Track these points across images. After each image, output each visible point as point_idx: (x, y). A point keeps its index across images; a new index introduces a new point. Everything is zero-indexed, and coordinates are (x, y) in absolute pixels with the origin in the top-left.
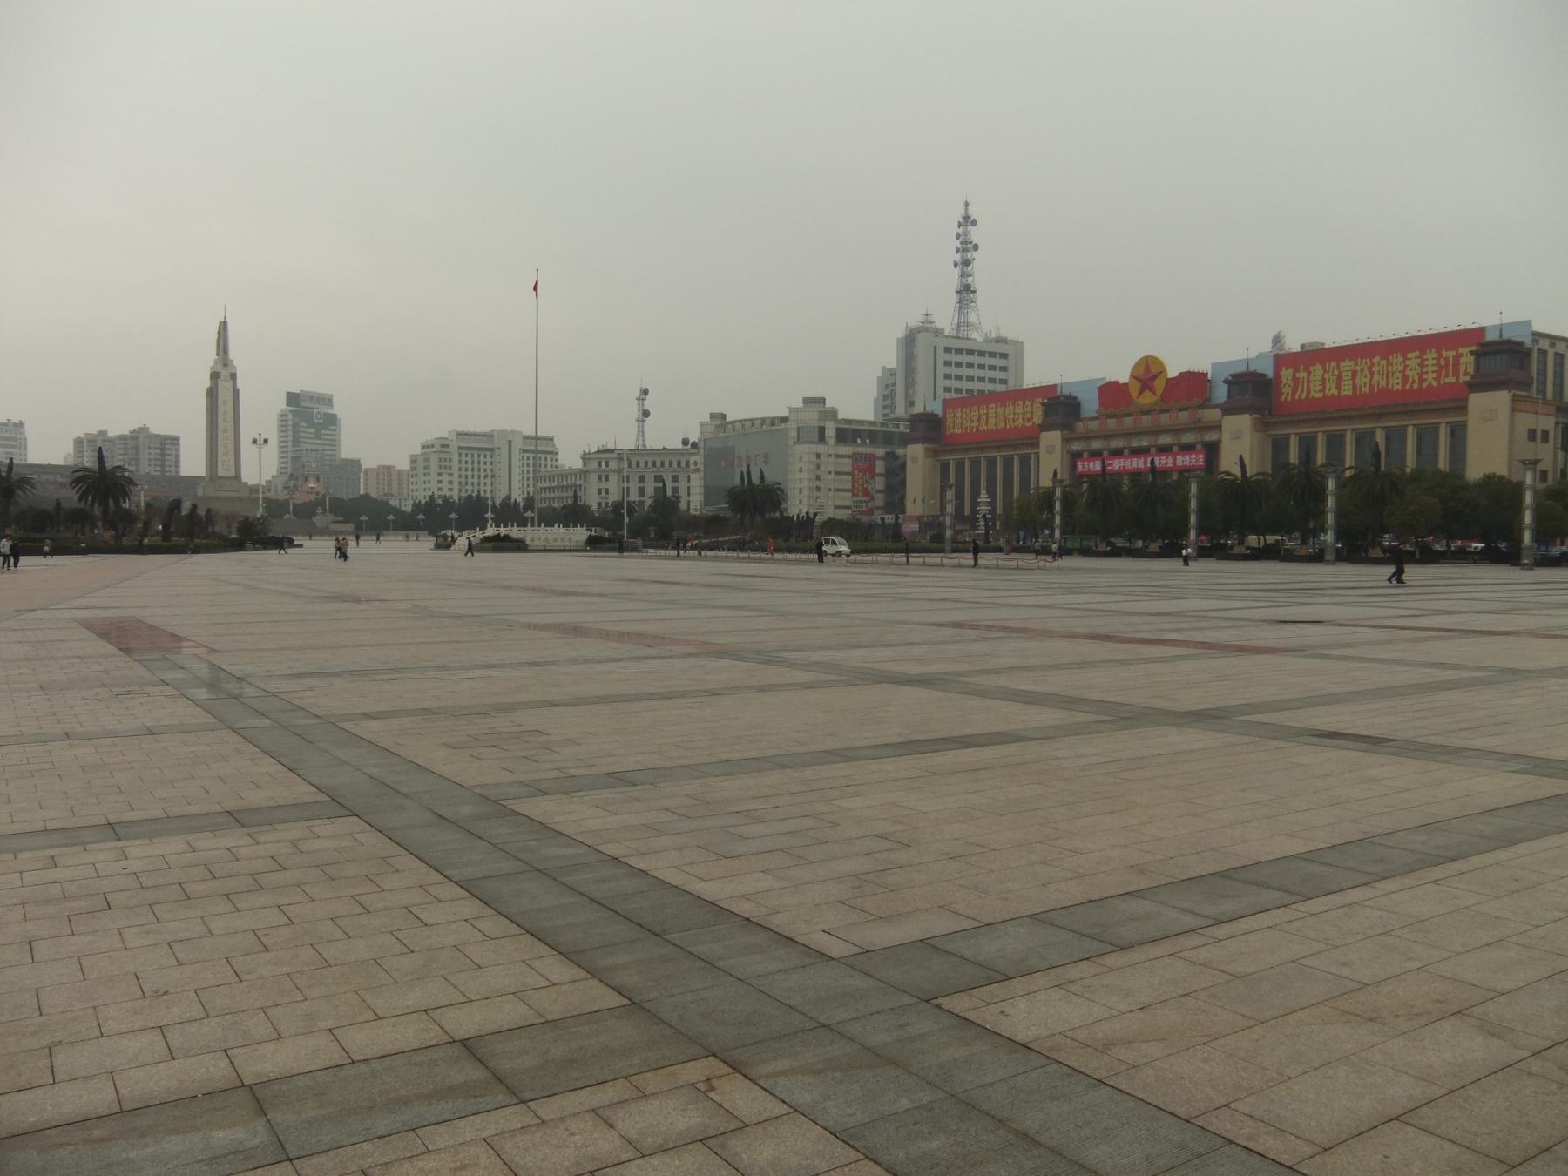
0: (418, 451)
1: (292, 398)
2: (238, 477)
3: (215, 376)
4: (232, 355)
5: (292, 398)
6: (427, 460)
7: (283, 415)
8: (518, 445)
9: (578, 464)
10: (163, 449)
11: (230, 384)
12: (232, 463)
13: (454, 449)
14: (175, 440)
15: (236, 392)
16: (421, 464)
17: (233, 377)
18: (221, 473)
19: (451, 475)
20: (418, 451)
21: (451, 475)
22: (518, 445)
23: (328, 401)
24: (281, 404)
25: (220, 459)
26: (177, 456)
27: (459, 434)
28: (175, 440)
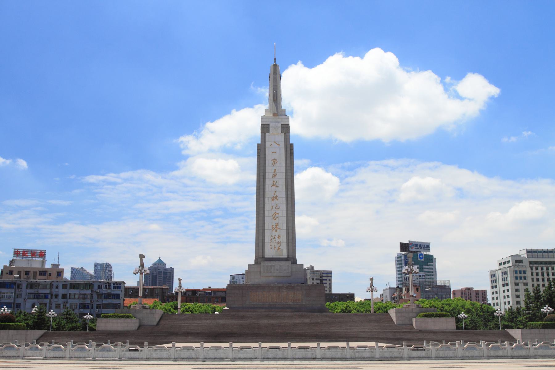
0: (497, 267)
1: (404, 247)
2: (291, 259)
3: (265, 128)
4: (285, 103)
5: (404, 247)
6: (504, 273)
7: (399, 257)
10: (321, 280)
11: (281, 138)
12: (284, 239)
13: (526, 263)
14: (328, 274)
15: (289, 150)
16: (499, 277)
17: (286, 128)
18: (269, 253)
19: (526, 284)
20: (497, 267)
21: (526, 284)
23: (427, 247)
24: (398, 250)
25: (267, 233)
27: (528, 252)
28: (328, 274)
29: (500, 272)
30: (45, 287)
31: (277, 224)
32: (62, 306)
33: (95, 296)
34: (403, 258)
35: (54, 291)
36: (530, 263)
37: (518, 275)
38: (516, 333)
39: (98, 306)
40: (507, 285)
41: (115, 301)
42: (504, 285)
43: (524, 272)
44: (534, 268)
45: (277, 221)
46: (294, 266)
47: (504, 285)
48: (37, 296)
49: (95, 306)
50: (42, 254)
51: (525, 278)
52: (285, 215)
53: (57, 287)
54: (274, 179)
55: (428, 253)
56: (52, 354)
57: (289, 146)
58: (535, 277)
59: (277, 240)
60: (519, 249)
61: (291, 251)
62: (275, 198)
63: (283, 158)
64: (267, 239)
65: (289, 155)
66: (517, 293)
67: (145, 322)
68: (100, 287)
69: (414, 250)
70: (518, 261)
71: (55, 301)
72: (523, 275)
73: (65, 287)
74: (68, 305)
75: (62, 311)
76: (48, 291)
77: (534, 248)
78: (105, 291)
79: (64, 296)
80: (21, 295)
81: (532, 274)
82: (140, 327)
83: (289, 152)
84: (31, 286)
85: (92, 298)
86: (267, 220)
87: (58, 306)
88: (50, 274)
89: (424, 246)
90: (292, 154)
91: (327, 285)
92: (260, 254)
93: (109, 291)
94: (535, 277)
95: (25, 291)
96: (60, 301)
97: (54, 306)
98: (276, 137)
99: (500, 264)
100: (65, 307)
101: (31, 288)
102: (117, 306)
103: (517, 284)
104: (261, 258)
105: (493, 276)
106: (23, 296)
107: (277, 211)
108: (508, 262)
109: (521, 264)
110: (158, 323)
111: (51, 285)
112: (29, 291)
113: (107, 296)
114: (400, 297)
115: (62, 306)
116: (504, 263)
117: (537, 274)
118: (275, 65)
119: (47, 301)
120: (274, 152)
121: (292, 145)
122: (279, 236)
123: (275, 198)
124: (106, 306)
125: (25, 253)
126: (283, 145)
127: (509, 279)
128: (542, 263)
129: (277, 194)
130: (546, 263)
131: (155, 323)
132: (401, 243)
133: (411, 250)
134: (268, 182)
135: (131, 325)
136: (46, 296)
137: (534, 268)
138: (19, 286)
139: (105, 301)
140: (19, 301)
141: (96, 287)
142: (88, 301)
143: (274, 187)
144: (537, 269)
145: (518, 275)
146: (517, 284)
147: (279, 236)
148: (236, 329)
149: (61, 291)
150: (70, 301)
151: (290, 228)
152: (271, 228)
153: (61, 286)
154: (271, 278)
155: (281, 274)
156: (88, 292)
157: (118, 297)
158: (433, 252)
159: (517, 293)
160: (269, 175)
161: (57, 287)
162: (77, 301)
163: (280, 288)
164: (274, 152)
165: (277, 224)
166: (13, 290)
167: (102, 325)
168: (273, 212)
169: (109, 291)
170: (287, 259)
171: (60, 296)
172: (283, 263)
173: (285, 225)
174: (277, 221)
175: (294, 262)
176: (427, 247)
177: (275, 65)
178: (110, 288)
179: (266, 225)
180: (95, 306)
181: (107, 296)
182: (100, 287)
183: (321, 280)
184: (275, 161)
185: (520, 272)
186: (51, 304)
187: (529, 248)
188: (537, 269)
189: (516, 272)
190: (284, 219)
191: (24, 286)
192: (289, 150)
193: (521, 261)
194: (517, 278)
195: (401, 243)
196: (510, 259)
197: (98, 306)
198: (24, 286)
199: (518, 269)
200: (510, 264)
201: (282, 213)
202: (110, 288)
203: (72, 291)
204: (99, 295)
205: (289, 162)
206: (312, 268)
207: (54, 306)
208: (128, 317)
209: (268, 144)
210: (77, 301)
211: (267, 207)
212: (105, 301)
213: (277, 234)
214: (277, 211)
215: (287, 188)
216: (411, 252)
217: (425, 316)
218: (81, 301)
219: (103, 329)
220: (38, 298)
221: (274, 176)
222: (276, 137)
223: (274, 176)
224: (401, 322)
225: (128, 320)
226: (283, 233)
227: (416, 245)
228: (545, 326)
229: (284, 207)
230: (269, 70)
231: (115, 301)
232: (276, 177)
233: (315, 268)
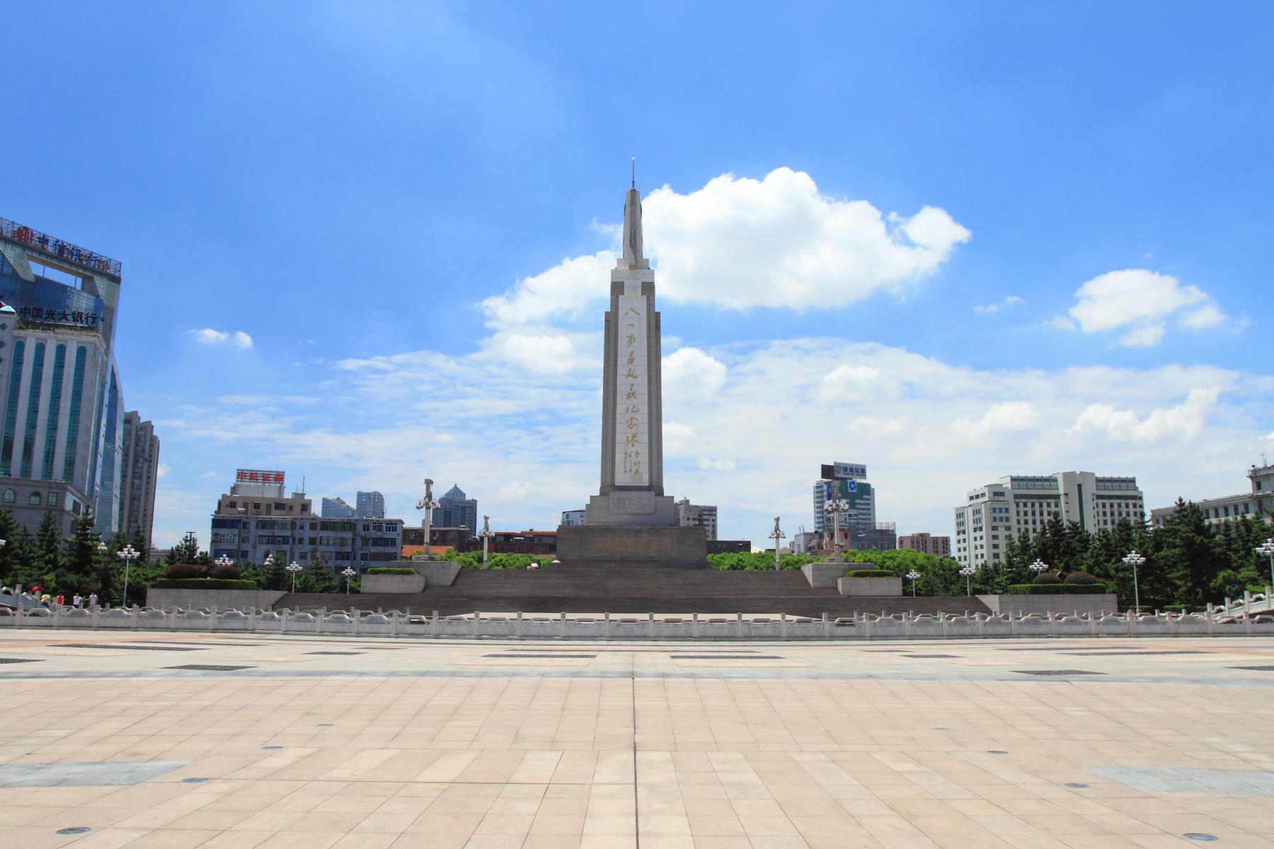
0: (966, 502)
1: (827, 471)
2: (656, 487)
3: (617, 288)
4: (648, 250)
5: (827, 471)
6: (977, 512)
7: (819, 487)
8: (1090, 490)
9: (1246, 488)
10: (701, 521)
11: (642, 303)
12: (644, 458)
13: (1009, 498)
14: (712, 511)
15: (654, 322)
16: (970, 517)
17: (649, 289)
18: (621, 479)
19: (1008, 528)
20: (966, 502)
21: (1008, 528)
22: (1090, 490)
23: (861, 471)
24: (817, 477)
25: (619, 449)
26: (714, 526)
27: (1013, 479)
28: (712, 511)
29: (970, 510)
30: (283, 526)
31: (634, 436)
32: (309, 556)
33: (359, 542)
34: (825, 488)
35: (298, 534)
36: (1016, 496)
37: (998, 515)
38: (991, 601)
39: (364, 557)
40: (981, 529)
41: (389, 550)
42: (975, 530)
43: (1007, 510)
44: (1021, 505)
45: (634, 430)
46: (660, 498)
47: (975, 530)
48: (272, 540)
49: (358, 557)
50: (279, 477)
51: (1007, 519)
52: (646, 420)
53: (302, 528)
54: (631, 366)
55: (863, 481)
56: (295, 626)
57: (653, 317)
58: (1022, 518)
59: (634, 459)
60: (1000, 476)
61: (655, 475)
62: (631, 395)
63: (644, 333)
64: (619, 457)
65: (653, 330)
66: (996, 542)
67: (434, 581)
68: (366, 528)
69: (841, 475)
70: (997, 493)
71: (298, 548)
72: (1004, 515)
73: (313, 526)
74: (318, 555)
75: (310, 563)
76: (288, 533)
77: (1022, 474)
78: (373, 534)
79: (312, 541)
80: (248, 538)
81: (1018, 513)
82: (426, 588)
83: (653, 326)
84: (263, 524)
85: (354, 543)
86: (619, 428)
87: (303, 556)
88: (291, 508)
89: (857, 470)
90: (658, 328)
91: (710, 529)
92: (609, 481)
93: (380, 534)
94: (1022, 518)
95: (254, 532)
96: (307, 548)
97: (297, 555)
98: (633, 302)
99: (971, 498)
100: (313, 557)
101: (263, 527)
102: (392, 557)
103: (995, 528)
104: (609, 487)
105: (960, 515)
106: (252, 540)
107: (636, 415)
108: (983, 495)
109: (1001, 498)
110: (454, 584)
111: (293, 524)
112: (261, 532)
113: (377, 542)
114: (820, 546)
115: (309, 556)
116: (977, 497)
117: (1026, 513)
118: (633, 191)
119: (287, 547)
120: (633, 324)
121: (658, 314)
122: (637, 453)
123: (631, 395)
124: (375, 557)
125: (253, 476)
126: (644, 314)
127: (984, 520)
128: (1032, 497)
129: (635, 388)
130: (1040, 497)
131: (449, 583)
132: (824, 467)
133: (837, 475)
134: (622, 371)
135: (412, 584)
136: (285, 540)
137: (1021, 505)
138: (245, 525)
139: (374, 550)
140: (245, 547)
141: (360, 528)
142: (349, 549)
143: (630, 379)
144: (1025, 505)
145: (998, 515)
146: (995, 528)
147: (637, 453)
148: (569, 592)
149: (308, 534)
150: (322, 548)
151: (654, 441)
152: (624, 440)
153: (307, 527)
154: (625, 518)
155: (640, 511)
156: (349, 535)
157: (392, 542)
158: (868, 480)
159: (996, 542)
160: (622, 360)
161: (302, 528)
162: (332, 549)
163: (638, 532)
164: (633, 324)
165: (634, 436)
166: (236, 531)
167: (370, 584)
168: (629, 416)
169: (380, 534)
170: (649, 488)
171: (307, 540)
172: (643, 494)
173: (646, 436)
174: (634, 430)
175: (660, 492)
176: (861, 471)
177: (633, 191)
178: (380, 530)
179: (618, 436)
180: (358, 557)
181: (377, 542)
182: (366, 528)
183: (701, 521)
184: (631, 339)
185: (1001, 510)
186: (292, 552)
187: (1015, 475)
188: (1025, 505)
189: (994, 510)
190: (646, 427)
191: (253, 525)
192: (653, 321)
193: (1002, 494)
194: (995, 519)
195: (824, 467)
196: (986, 491)
197: (364, 557)
198: (253, 525)
199: (997, 506)
200: (986, 499)
201: (642, 418)
202: (380, 530)
203: (324, 534)
204: (365, 541)
205: (653, 340)
206: (688, 501)
207: (297, 555)
208: (409, 573)
209: (621, 313)
210: (332, 549)
211: (619, 409)
212: (374, 550)
213: (634, 450)
214: (636, 415)
215: (649, 380)
216: (837, 479)
217: (857, 575)
218: (338, 549)
219: (372, 590)
220: (273, 542)
221: (631, 361)
222: (633, 302)
223: (631, 361)
224: (820, 585)
225: (408, 578)
226: (644, 449)
227: (845, 469)
228: (1035, 591)
229: (644, 409)
230: (623, 199)
231: (389, 550)
232: (635, 362)
233: (692, 503)
